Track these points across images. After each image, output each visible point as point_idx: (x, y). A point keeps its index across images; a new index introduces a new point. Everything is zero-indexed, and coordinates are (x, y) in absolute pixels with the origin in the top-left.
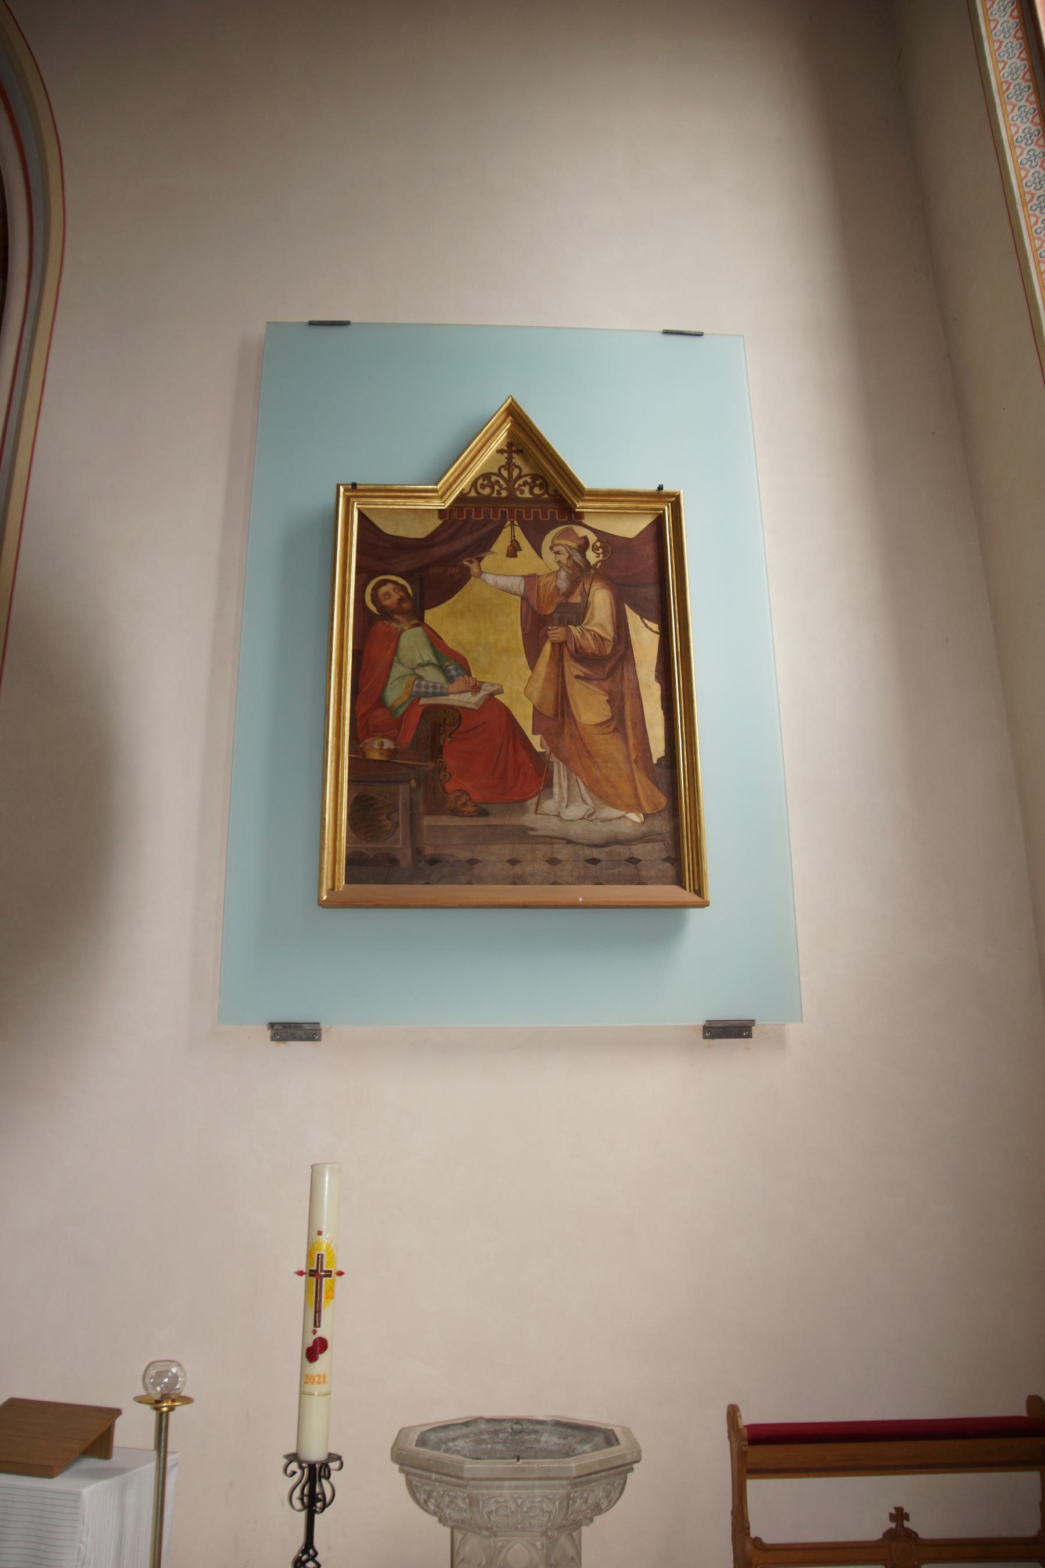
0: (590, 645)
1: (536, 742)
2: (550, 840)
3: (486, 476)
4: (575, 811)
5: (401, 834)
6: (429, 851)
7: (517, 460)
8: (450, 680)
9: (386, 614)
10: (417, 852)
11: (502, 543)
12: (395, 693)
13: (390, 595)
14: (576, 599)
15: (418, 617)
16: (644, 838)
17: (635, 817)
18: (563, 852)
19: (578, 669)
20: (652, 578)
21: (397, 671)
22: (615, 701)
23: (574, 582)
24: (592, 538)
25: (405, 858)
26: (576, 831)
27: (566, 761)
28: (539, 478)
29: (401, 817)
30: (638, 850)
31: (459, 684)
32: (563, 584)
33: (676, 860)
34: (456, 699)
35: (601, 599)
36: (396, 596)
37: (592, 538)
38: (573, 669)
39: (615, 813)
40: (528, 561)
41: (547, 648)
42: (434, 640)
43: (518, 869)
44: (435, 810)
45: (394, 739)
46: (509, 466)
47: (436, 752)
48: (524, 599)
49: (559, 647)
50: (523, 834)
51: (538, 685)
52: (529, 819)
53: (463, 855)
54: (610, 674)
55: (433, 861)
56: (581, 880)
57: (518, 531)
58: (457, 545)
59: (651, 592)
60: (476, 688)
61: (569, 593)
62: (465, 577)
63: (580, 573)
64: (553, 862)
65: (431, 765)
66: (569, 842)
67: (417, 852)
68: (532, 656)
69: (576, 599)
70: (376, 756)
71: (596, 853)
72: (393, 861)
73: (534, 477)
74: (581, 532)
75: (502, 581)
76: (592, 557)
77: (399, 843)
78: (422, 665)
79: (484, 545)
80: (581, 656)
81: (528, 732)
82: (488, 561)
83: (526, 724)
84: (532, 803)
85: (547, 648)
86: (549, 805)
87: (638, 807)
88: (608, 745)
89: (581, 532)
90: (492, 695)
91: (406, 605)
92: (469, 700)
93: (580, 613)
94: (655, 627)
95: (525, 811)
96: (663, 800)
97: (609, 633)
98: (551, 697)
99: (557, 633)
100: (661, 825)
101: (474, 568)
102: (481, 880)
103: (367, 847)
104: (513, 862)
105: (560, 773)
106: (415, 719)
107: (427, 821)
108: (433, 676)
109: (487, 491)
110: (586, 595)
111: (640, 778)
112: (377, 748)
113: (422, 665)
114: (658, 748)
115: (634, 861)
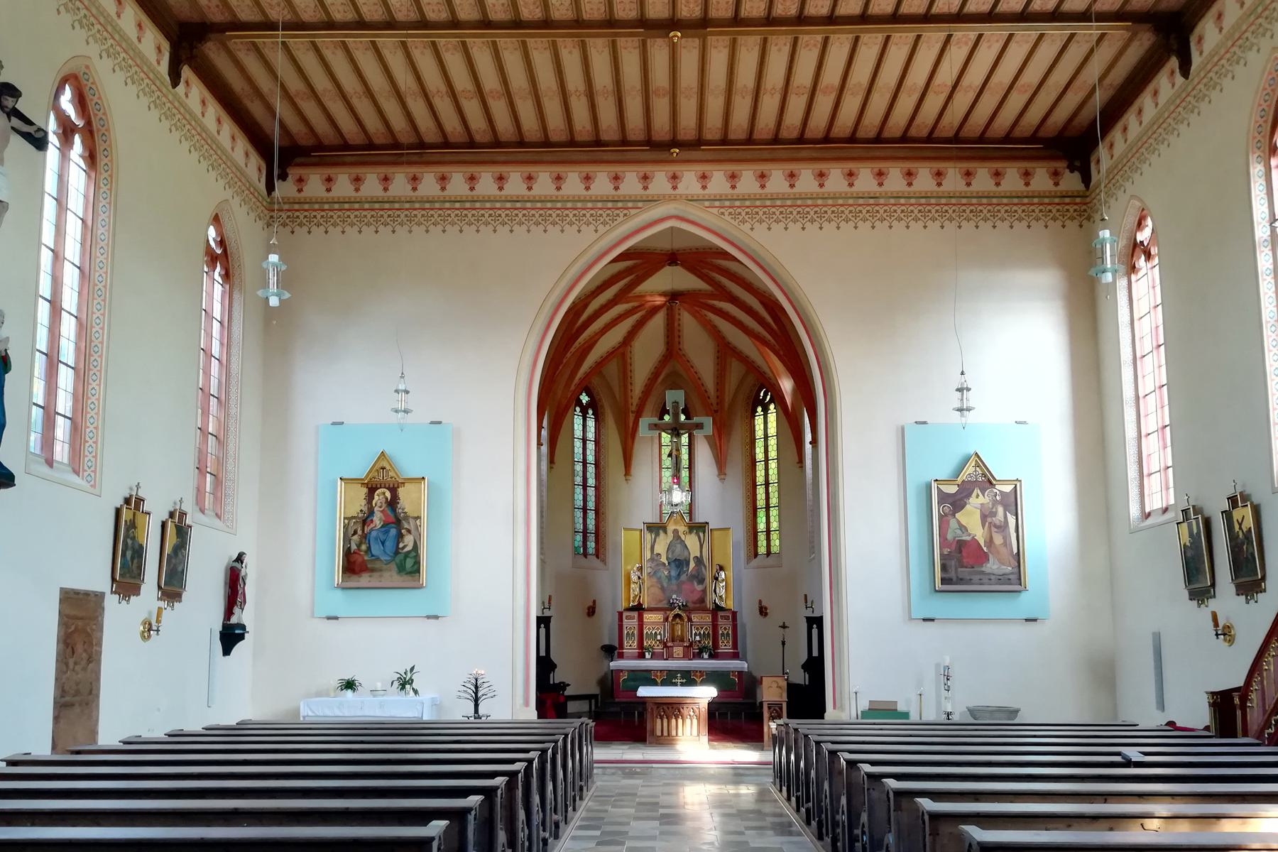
0: (998, 523)
1: (985, 549)
2: (989, 574)
3: (969, 474)
4: (995, 567)
5: (953, 572)
6: (960, 577)
7: (978, 469)
8: (963, 533)
9: (946, 515)
10: (957, 577)
11: (974, 494)
12: (950, 537)
13: (946, 509)
14: (994, 510)
15: (954, 515)
16: (1012, 573)
17: (1010, 568)
18: (993, 577)
19: (996, 530)
20: (1014, 504)
21: (950, 531)
22: (1005, 538)
23: (993, 505)
24: (998, 492)
25: (955, 579)
26: (995, 572)
27: (992, 554)
28: (984, 475)
29: (953, 569)
30: (1011, 577)
31: (965, 534)
32: (991, 506)
33: (1020, 579)
34: (964, 538)
35: (1000, 510)
36: (948, 510)
37: (998, 492)
38: (994, 529)
39: (1005, 567)
40: (982, 500)
41: (987, 523)
42: (959, 522)
43: (981, 581)
44: (962, 567)
45: (950, 548)
46: (976, 471)
47: (960, 552)
48: (981, 510)
49: (990, 523)
50: (983, 573)
51: (986, 532)
52: (983, 569)
53: (968, 578)
54: (1003, 530)
55: (961, 579)
56: (997, 584)
57: (979, 491)
58: (962, 495)
59: (1014, 508)
60: (969, 535)
61: (992, 508)
62: (965, 504)
63: (995, 503)
64: (990, 579)
65: (959, 555)
66: (994, 574)
67: (957, 577)
68: (983, 526)
69: (994, 510)
70: (946, 553)
71: (1000, 577)
72: (952, 580)
73: (983, 474)
74: (995, 491)
75: (976, 506)
76: (998, 498)
77: (952, 575)
78: (956, 529)
79: (969, 495)
80: (996, 526)
81: (983, 546)
82: (971, 500)
83: (982, 544)
84: (984, 565)
85: (987, 523)
86: (988, 565)
87: (1010, 566)
88: (1003, 550)
89: (995, 491)
90: (973, 537)
91: (951, 513)
92: (968, 538)
93: (994, 514)
94: (1015, 517)
95: (982, 567)
96: (1017, 564)
97: (1003, 520)
98: (988, 536)
99: (989, 520)
100: (1016, 570)
101: (967, 502)
102: (973, 584)
103: (946, 576)
104: (980, 580)
105: (991, 556)
106: (955, 543)
107: (960, 569)
108: (959, 532)
109: (970, 479)
110: (996, 509)
111: (1011, 558)
112: (946, 551)
113: (956, 529)
114: (1015, 551)
115: (1009, 579)
